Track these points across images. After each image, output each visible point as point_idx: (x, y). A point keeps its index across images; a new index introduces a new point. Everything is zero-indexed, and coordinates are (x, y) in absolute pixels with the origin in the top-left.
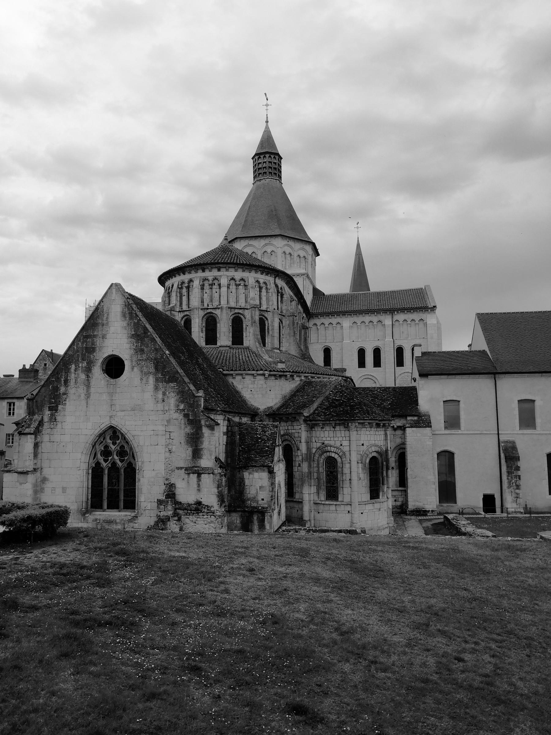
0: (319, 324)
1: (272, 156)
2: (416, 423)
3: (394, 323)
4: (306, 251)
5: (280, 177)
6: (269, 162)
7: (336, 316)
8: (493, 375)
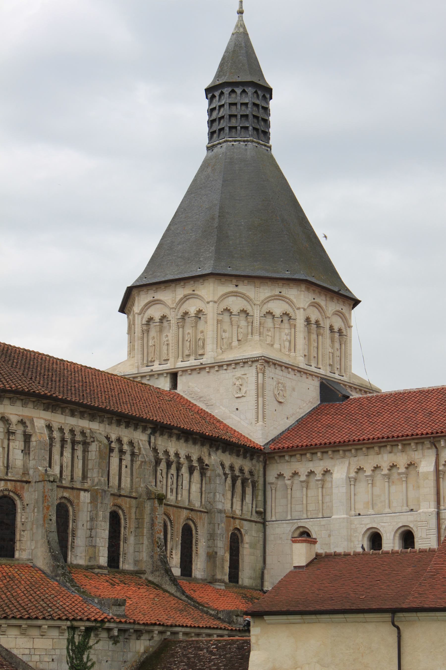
0: (287, 474)
1: (239, 91)
4: (290, 302)
5: (266, 134)
6: (231, 104)
7: (353, 451)
8: (388, 617)
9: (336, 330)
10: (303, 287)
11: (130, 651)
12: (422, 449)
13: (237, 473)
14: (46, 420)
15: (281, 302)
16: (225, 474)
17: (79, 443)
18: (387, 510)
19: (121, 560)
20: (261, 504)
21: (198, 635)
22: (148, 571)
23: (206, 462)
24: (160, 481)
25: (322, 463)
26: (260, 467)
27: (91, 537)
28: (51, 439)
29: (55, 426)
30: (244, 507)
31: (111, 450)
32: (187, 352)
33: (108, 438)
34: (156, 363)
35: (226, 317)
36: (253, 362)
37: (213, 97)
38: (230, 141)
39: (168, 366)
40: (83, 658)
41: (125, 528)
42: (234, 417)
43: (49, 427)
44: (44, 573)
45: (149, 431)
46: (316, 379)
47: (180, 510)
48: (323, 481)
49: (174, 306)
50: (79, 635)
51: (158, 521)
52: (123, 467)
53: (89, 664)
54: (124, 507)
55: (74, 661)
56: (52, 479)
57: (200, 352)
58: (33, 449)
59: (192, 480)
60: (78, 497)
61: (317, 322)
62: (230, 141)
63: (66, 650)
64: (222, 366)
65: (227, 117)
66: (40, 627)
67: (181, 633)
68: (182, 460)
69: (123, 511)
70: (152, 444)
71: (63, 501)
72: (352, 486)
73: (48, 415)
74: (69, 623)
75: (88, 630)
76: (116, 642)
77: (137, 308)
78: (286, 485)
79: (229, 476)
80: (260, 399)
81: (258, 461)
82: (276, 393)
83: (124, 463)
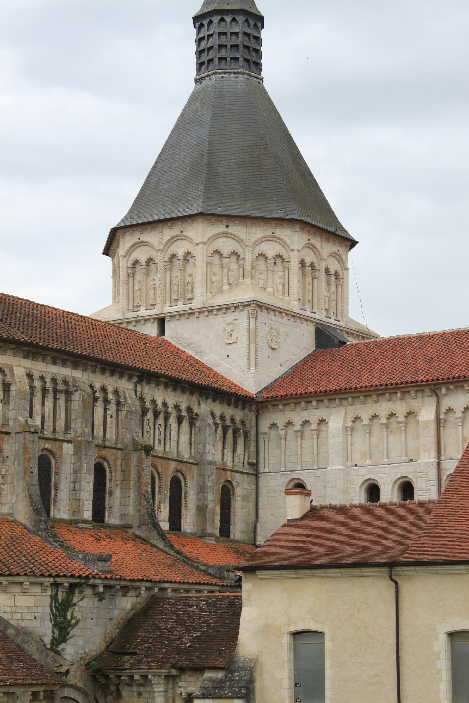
0: (281, 423)
1: (228, 19)
2: (215, 688)
3: (442, 416)
4: (283, 243)
5: (258, 65)
6: (220, 34)
7: (350, 399)
8: (385, 570)
9: (332, 272)
10: (297, 227)
11: (116, 608)
12: (422, 397)
13: (228, 423)
14: (26, 368)
15: (274, 243)
16: (216, 424)
17: (61, 392)
18: (385, 461)
19: (107, 513)
20: (253, 455)
21: (188, 591)
22: (135, 525)
23: (196, 411)
24: (147, 432)
25: (317, 412)
26: (252, 416)
27: (74, 490)
28: (32, 388)
29: (36, 374)
30: (236, 458)
31: (96, 400)
32: (175, 297)
33: (91, 387)
34: (143, 309)
35: (216, 260)
36: (244, 306)
37: (202, 25)
38: (220, 73)
39: (156, 311)
40: (67, 616)
41: (110, 480)
42: (225, 364)
43: (30, 376)
44: (26, 528)
45: (135, 380)
46: (311, 325)
47: (168, 461)
48: (318, 430)
49: (161, 248)
50: (63, 592)
51: (145, 473)
52: (108, 417)
53: (73, 621)
54: (109, 459)
55: (58, 618)
56: (33, 430)
57: (189, 296)
58: (12, 399)
59: (181, 430)
60: (61, 448)
61: (312, 265)
62: (220, 73)
63: (49, 608)
64: (212, 311)
65: (216, 47)
66: (21, 583)
67: (169, 590)
68: (170, 410)
69: (108, 463)
70: (138, 393)
71: (45, 452)
72: (349, 436)
73: (28, 363)
74: (52, 580)
75: (72, 587)
76: (101, 599)
77: (121, 251)
78: (279, 436)
79: (220, 426)
80: (252, 345)
81: (250, 410)
82: (269, 339)
83: (109, 412)
